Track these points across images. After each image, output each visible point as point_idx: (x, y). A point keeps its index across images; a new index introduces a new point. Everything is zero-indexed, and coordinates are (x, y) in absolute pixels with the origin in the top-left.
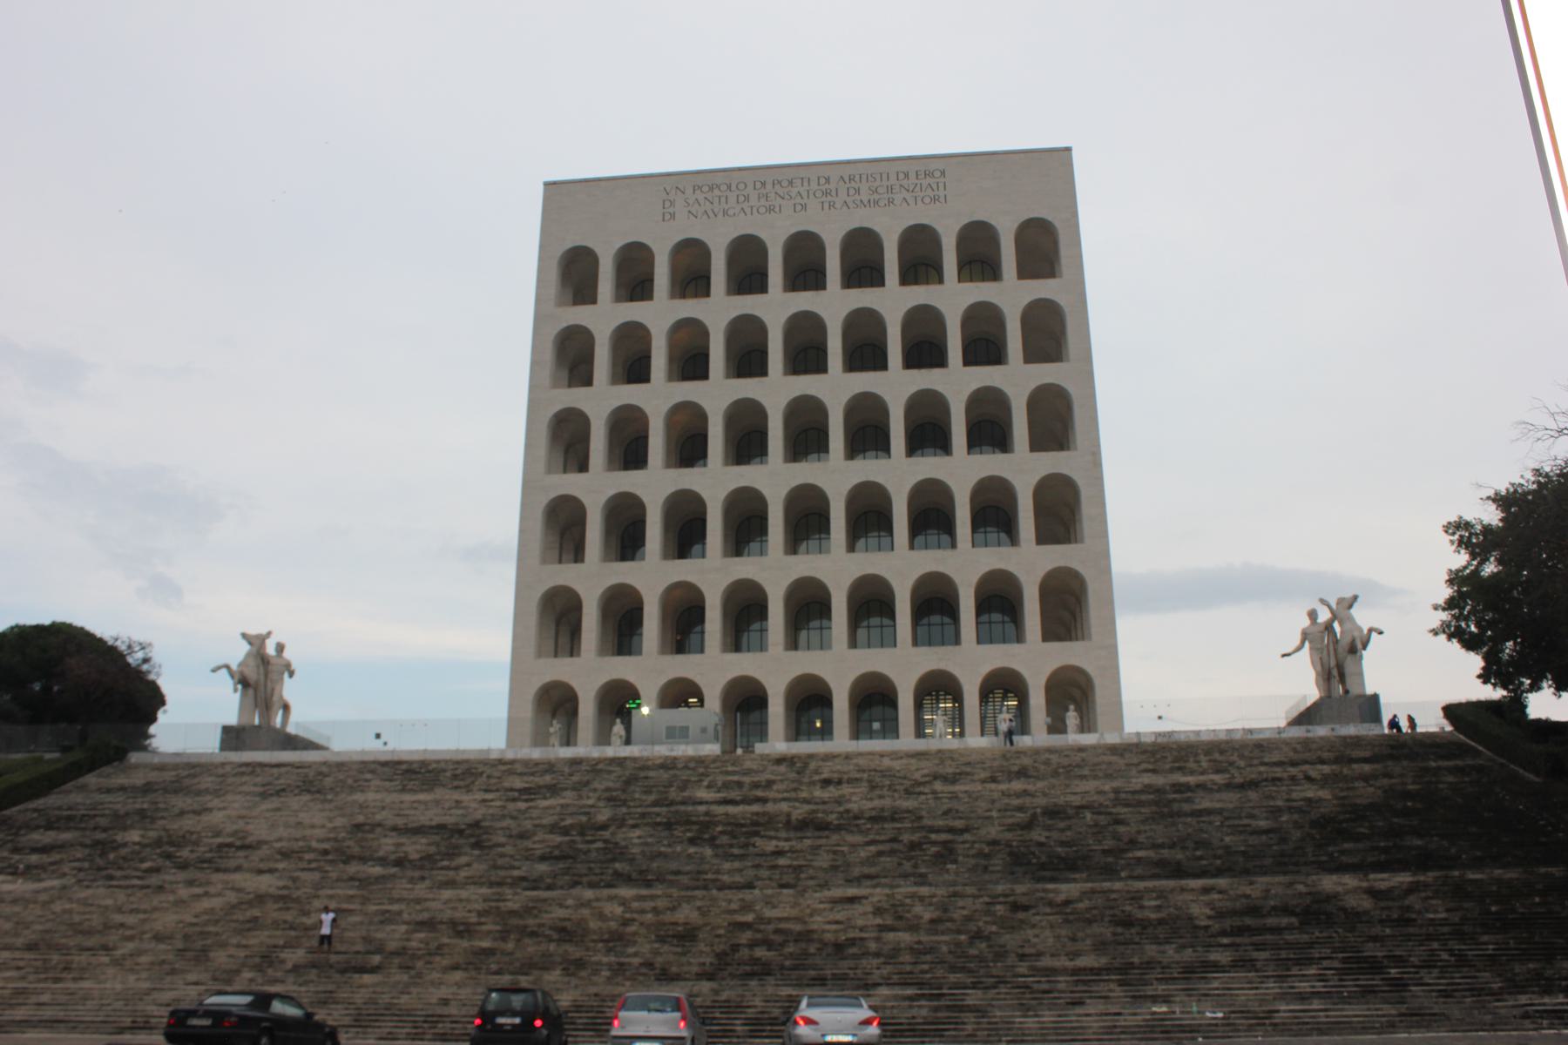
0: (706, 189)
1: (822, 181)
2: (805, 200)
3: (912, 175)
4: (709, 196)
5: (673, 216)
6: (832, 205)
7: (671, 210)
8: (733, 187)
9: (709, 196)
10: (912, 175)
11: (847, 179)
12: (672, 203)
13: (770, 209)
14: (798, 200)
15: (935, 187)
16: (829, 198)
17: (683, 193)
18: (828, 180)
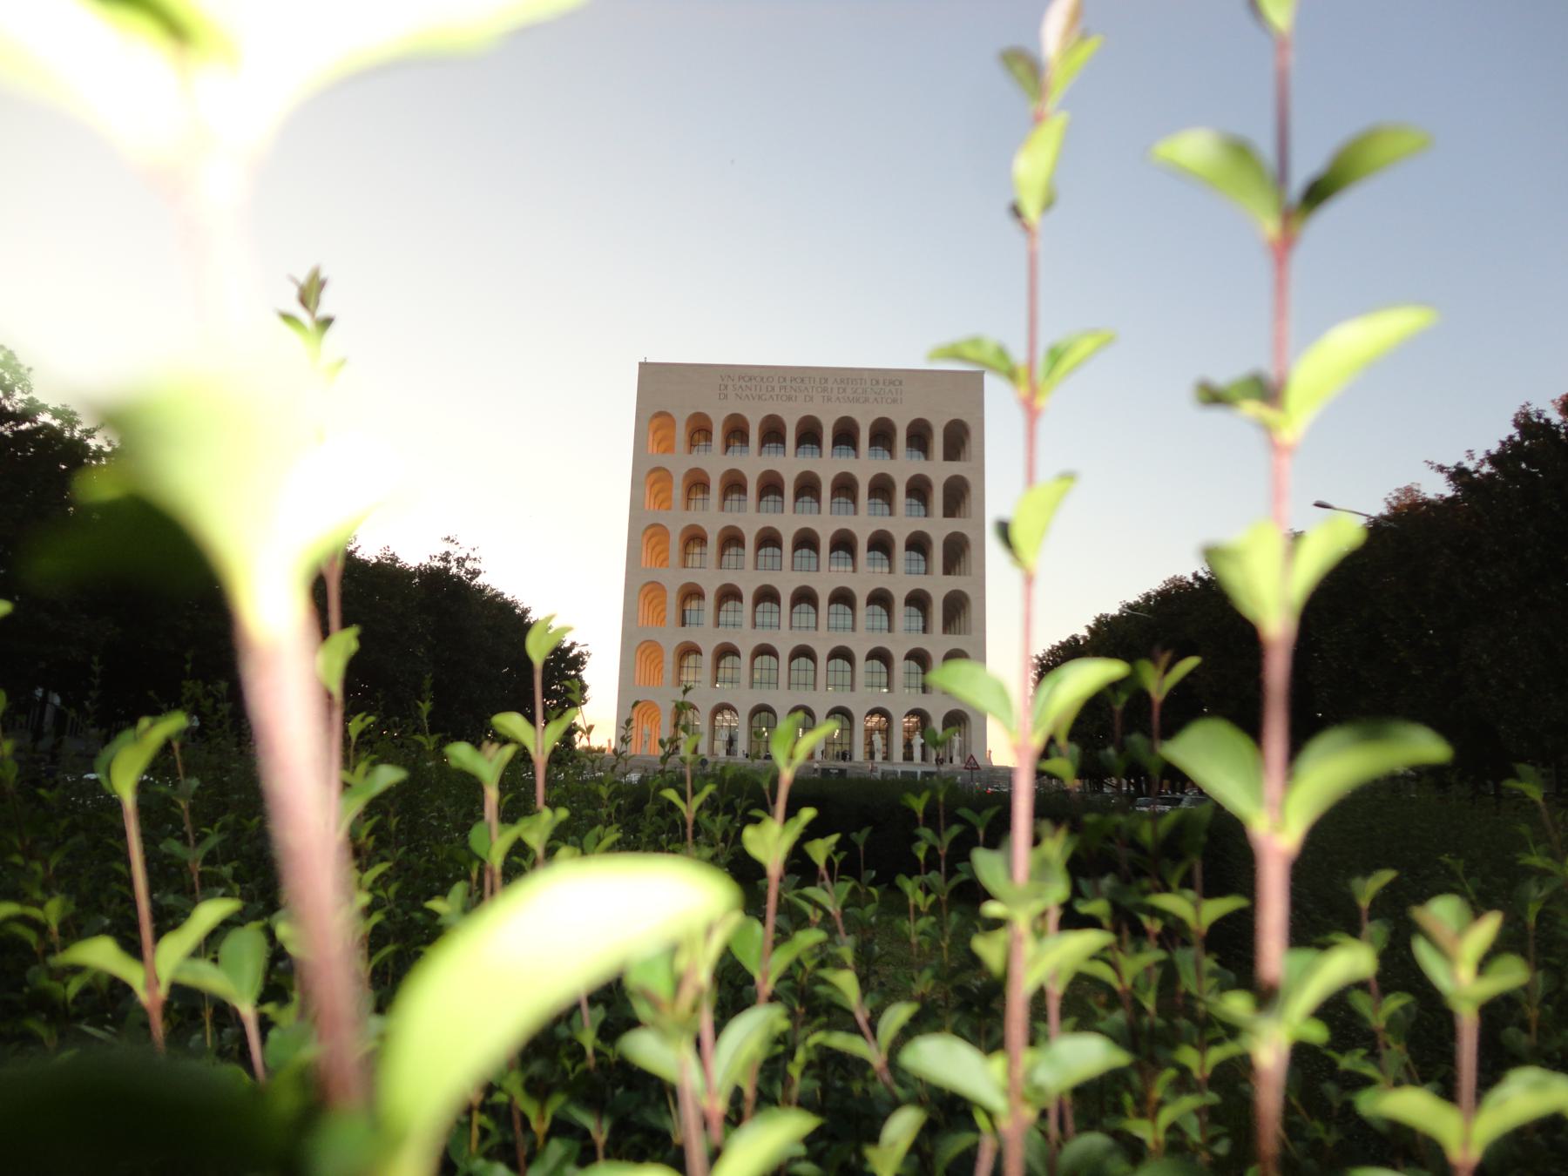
0: (747, 379)
1: (823, 381)
2: (811, 394)
3: (881, 382)
4: (749, 384)
5: (726, 397)
6: (829, 400)
7: (725, 392)
8: (765, 380)
9: (749, 384)
10: (881, 382)
11: (839, 381)
12: (726, 387)
13: (789, 398)
14: (806, 393)
15: (894, 391)
16: (826, 394)
17: (733, 380)
18: (826, 380)
